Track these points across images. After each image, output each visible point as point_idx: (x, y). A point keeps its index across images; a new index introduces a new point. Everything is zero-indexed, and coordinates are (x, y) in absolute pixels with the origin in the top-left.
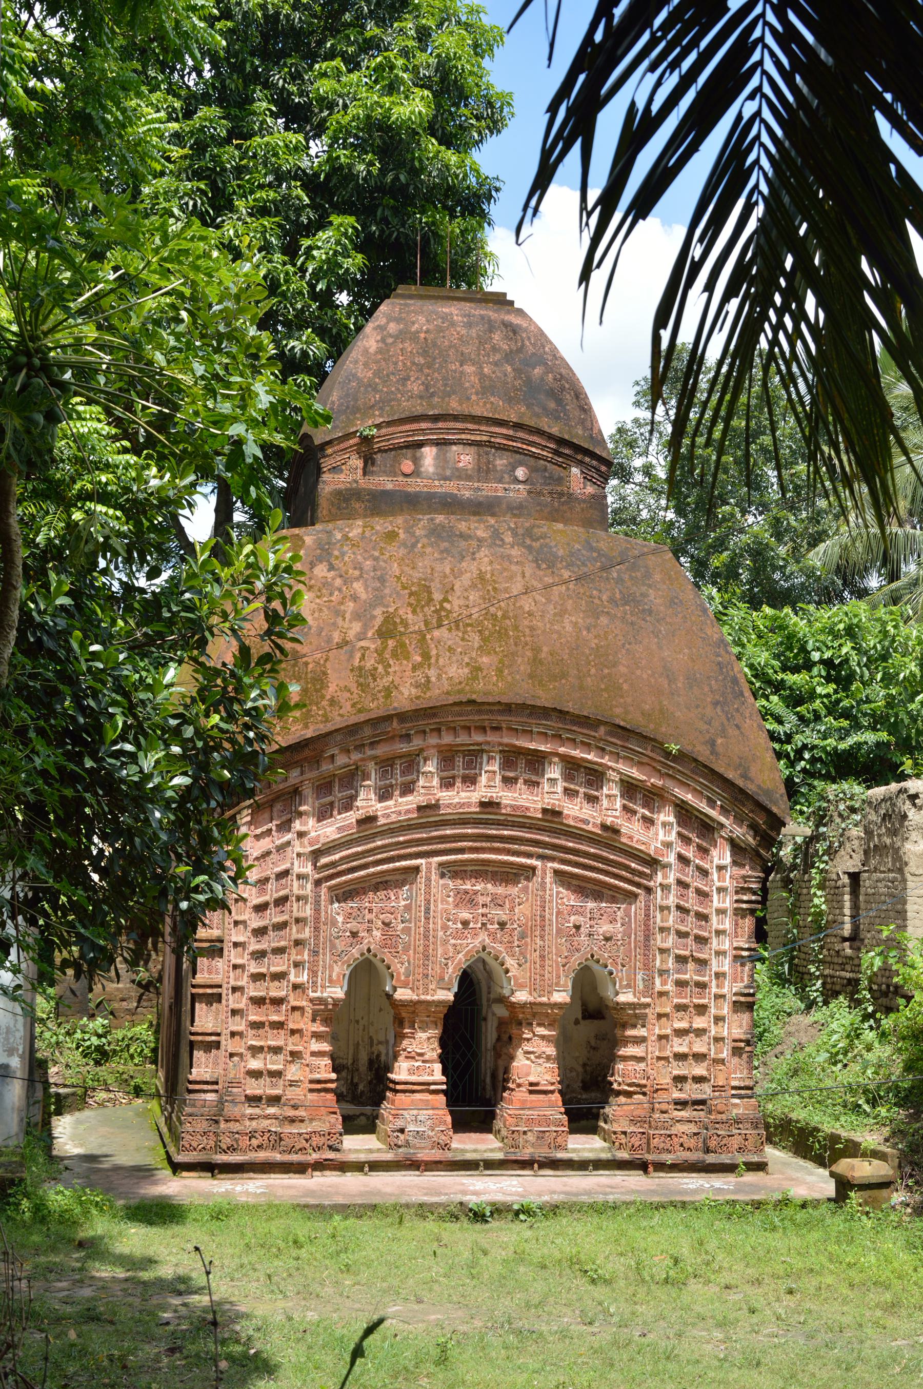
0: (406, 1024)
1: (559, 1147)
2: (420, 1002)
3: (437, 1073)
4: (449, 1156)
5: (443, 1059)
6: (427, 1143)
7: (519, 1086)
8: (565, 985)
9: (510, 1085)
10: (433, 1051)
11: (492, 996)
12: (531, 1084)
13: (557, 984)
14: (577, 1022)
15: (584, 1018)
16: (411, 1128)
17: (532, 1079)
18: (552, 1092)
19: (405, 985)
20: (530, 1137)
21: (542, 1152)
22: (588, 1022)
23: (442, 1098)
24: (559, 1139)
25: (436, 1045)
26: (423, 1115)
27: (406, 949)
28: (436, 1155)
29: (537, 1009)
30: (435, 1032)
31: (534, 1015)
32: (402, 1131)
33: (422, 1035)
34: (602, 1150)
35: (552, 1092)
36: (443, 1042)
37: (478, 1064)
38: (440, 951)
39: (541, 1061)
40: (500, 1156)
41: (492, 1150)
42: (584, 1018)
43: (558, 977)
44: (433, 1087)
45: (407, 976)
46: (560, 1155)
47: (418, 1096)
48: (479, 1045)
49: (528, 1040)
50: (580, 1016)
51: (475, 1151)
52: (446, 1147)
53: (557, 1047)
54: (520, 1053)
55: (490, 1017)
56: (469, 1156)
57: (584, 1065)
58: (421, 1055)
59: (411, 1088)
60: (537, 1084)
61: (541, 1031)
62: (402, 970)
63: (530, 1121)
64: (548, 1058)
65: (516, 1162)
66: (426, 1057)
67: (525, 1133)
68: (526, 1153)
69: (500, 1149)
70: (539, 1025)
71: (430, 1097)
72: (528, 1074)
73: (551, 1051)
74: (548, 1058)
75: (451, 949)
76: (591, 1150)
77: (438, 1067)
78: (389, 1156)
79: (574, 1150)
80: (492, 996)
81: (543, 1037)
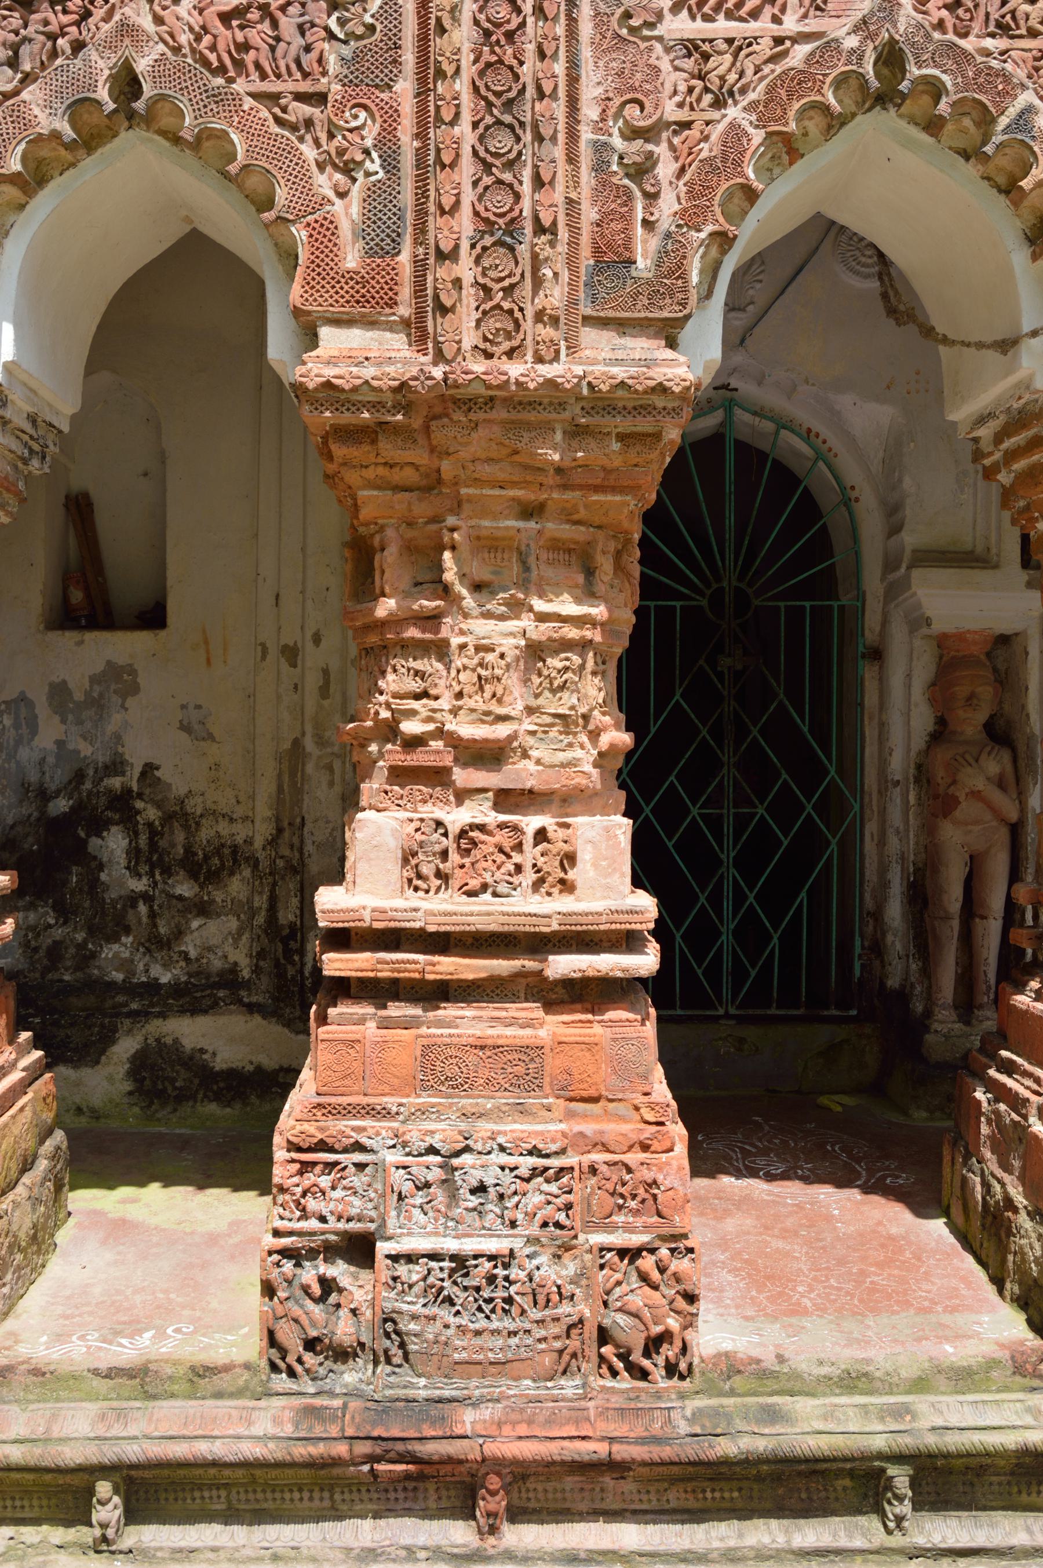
0: (390, 561)
2: (455, 403)
3: (600, 874)
4: (679, 1420)
5: (640, 782)
6: (532, 1334)
10: (570, 731)
11: (909, 540)
16: (413, 1233)
19: (366, 304)
23: (637, 1030)
25: (593, 692)
26: (516, 1127)
27: (370, 72)
28: (588, 1415)
30: (582, 612)
32: (359, 1249)
33: (484, 629)
36: (640, 682)
37: (850, 846)
38: (590, 91)
41: (965, 1378)
44: (563, 965)
45: (381, 246)
47: (466, 1022)
48: (851, 767)
51: (853, 1381)
52: (656, 1356)
55: (898, 633)
56: (818, 1426)
58: (489, 755)
59: (427, 970)
62: (348, 213)
66: (521, 773)
71: (550, 1027)
75: (673, 77)
77: (604, 838)
78: (257, 1428)
80: (909, 540)
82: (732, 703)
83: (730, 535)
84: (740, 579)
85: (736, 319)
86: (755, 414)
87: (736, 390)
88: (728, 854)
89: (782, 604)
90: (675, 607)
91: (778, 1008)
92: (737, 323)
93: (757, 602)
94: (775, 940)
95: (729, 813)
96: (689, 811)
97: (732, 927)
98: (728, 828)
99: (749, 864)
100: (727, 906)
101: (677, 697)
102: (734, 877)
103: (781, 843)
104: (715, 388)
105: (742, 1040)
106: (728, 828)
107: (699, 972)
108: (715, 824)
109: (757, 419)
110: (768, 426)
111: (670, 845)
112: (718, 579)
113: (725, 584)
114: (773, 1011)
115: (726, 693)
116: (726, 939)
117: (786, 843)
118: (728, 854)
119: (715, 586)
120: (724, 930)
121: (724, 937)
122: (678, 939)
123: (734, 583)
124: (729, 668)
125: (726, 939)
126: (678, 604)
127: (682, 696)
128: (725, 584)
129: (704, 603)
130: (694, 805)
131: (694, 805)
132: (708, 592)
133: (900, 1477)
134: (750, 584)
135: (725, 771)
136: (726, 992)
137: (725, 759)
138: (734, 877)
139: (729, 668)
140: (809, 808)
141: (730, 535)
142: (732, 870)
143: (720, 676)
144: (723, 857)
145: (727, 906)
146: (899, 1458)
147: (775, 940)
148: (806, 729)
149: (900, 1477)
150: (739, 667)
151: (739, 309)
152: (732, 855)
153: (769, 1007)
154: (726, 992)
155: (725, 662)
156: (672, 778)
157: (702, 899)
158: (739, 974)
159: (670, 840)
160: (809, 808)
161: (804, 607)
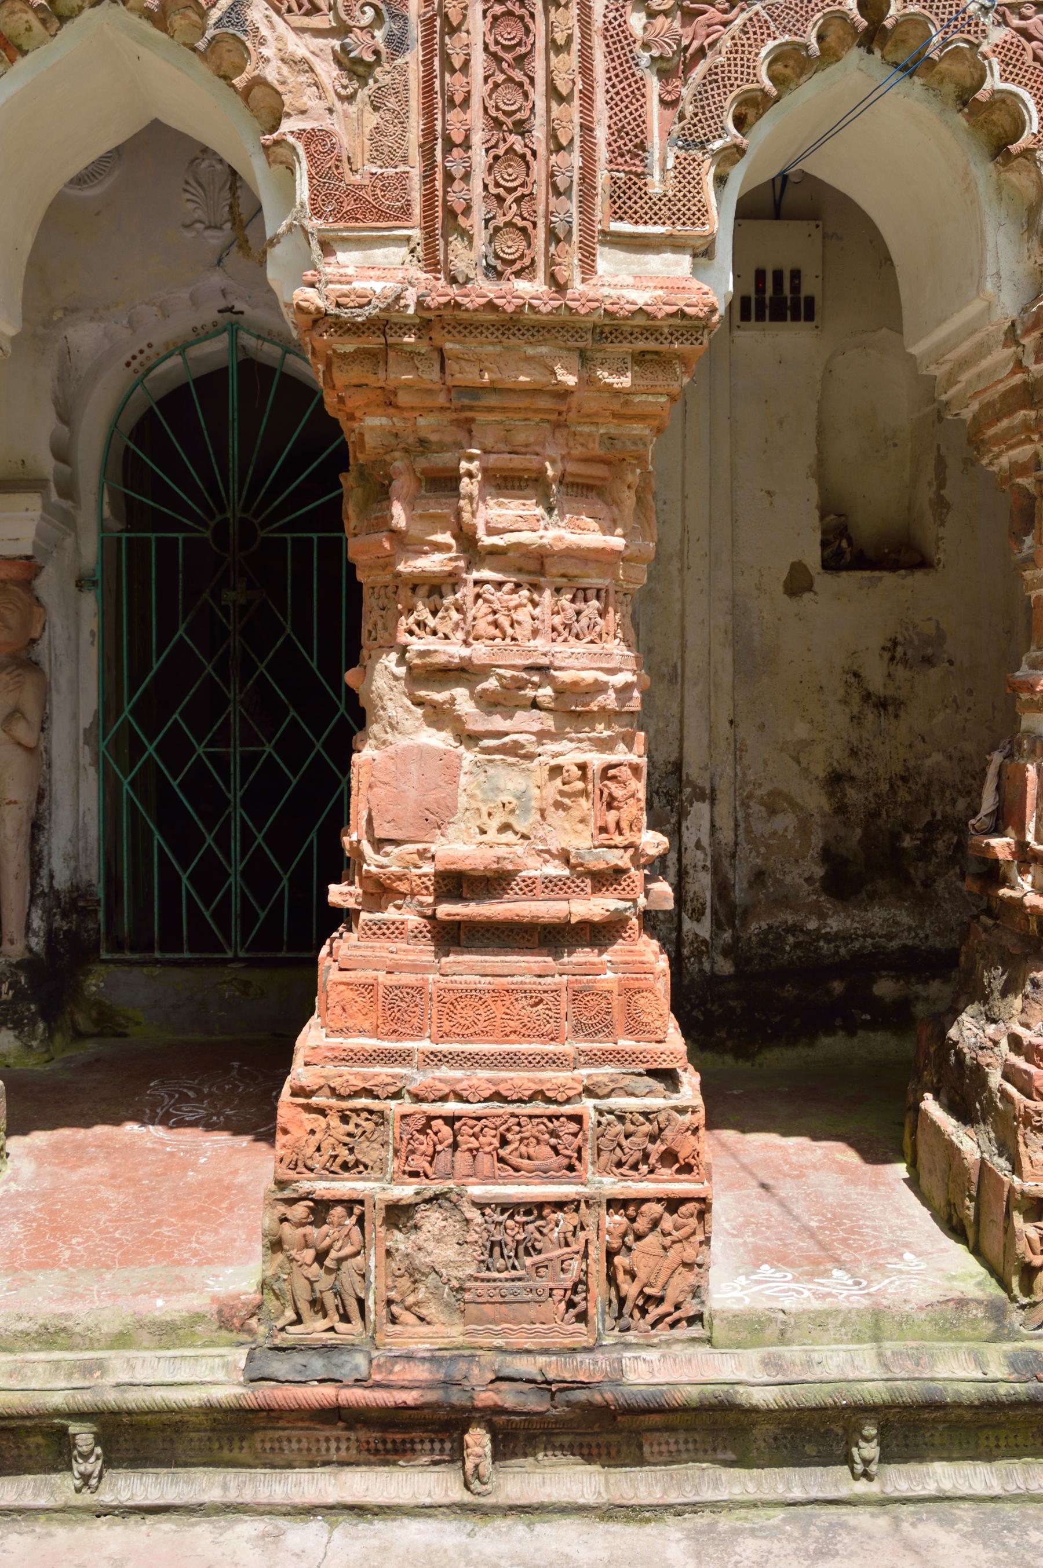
1: (644, 1309)
7: (381, 892)
8: (684, 206)
9: (338, 894)
12: (455, 884)
13: (628, 197)
14: (798, 583)
15: (832, 563)
17: (461, 848)
18: (600, 933)
20: (439, 1243)
21: (531, 1348)
22: (850, 580)
24: (645, 1258)
29: (479, 365)
31: (465, 406)
34: (950, 1316)
35: (600, 933)
39: (524, 725)
40: (211, 1376)
41: (169, 1334)
42: (832, 563)
43: (631, 146)
46: (656, 1368)
49: (436, 588)
50: (813, 558)
53: (642, 637)
54: (384, 679)
57: (836, 780)
60: (494, 882)
61: (509, 520)
63: (439, 1133)
64: (573, 707)
65: (334, 1415)
67: (398, 1215)
68: (406, 1357)
69: (230, 1321)
70: (504, 482)
72: (436, 819)
73: (602, 658)
74: (573, 707)
76: (875, 1325)
79: (753, 1329)
81: (533, 568)
82: (238, 638)
83: (233, 465)
84: (245, 509)
85: (213, 237)
86: (259, 337)
87: (242, 313)
88: (235, 794)
89: (288, 536)
90: (177, 539)
91: (289, 950)
92: (214, 242)
93: (262, 534)
94: (285, 882)
95: (236, 751)
96: (194, 750)
97: (240, 868)
98: (235, 769)
99: (257, 803)
100: (235, 846)
101: (181, 632)
102: (242, 817)
103: (290, 782)
104: (220, 311)
105: (247, 984)
106: (235, 769)
107: (207, 915)
108: (221, 763)
109: (260, 342)
110: (277, 351)
111: (175, 784)
112: (222, 510)
113: (229, 515)
114: (283, 954)
115: (231, 628)
116: (235, 881)
117: (294, 782)
118: (235, 794)
119: (219, 517)
120: (231, 871)
121: (232, 879)
122: (185, 881)
123: (239, 514)
124: (234, 602)
125: (235, 881)
126: (181, 536)
127: (186, 631)
128: (229, 515)
129: (208, 534)
130: (200, 744)
131: (200, 744)
132: (212, 524)
133: (83, 1435)
134: (256, 515)
135: (231, 708)
136: (235, 935)
137: (231, 696)
138: (242, 817)
139: (234, 602)
140: (318, 746)
141: (233, 465)
142: (240, 810)
143: (225, 610)
144: (230, 796)
145: (235, 846)
146: (80, 1415)
147: (285, 882)
148: (314, 665)
149: (83, 1435)
150: (242, 601)
151: (216, 227)
152: (239, 794)
153: (280, 950)
154: (235, 935)
155: (228, 596)
156: (176, 716)
157: (209, 840)
158: (248, 916)
159: (175, 779)
160: (318, 746)
161: (311, 539)
